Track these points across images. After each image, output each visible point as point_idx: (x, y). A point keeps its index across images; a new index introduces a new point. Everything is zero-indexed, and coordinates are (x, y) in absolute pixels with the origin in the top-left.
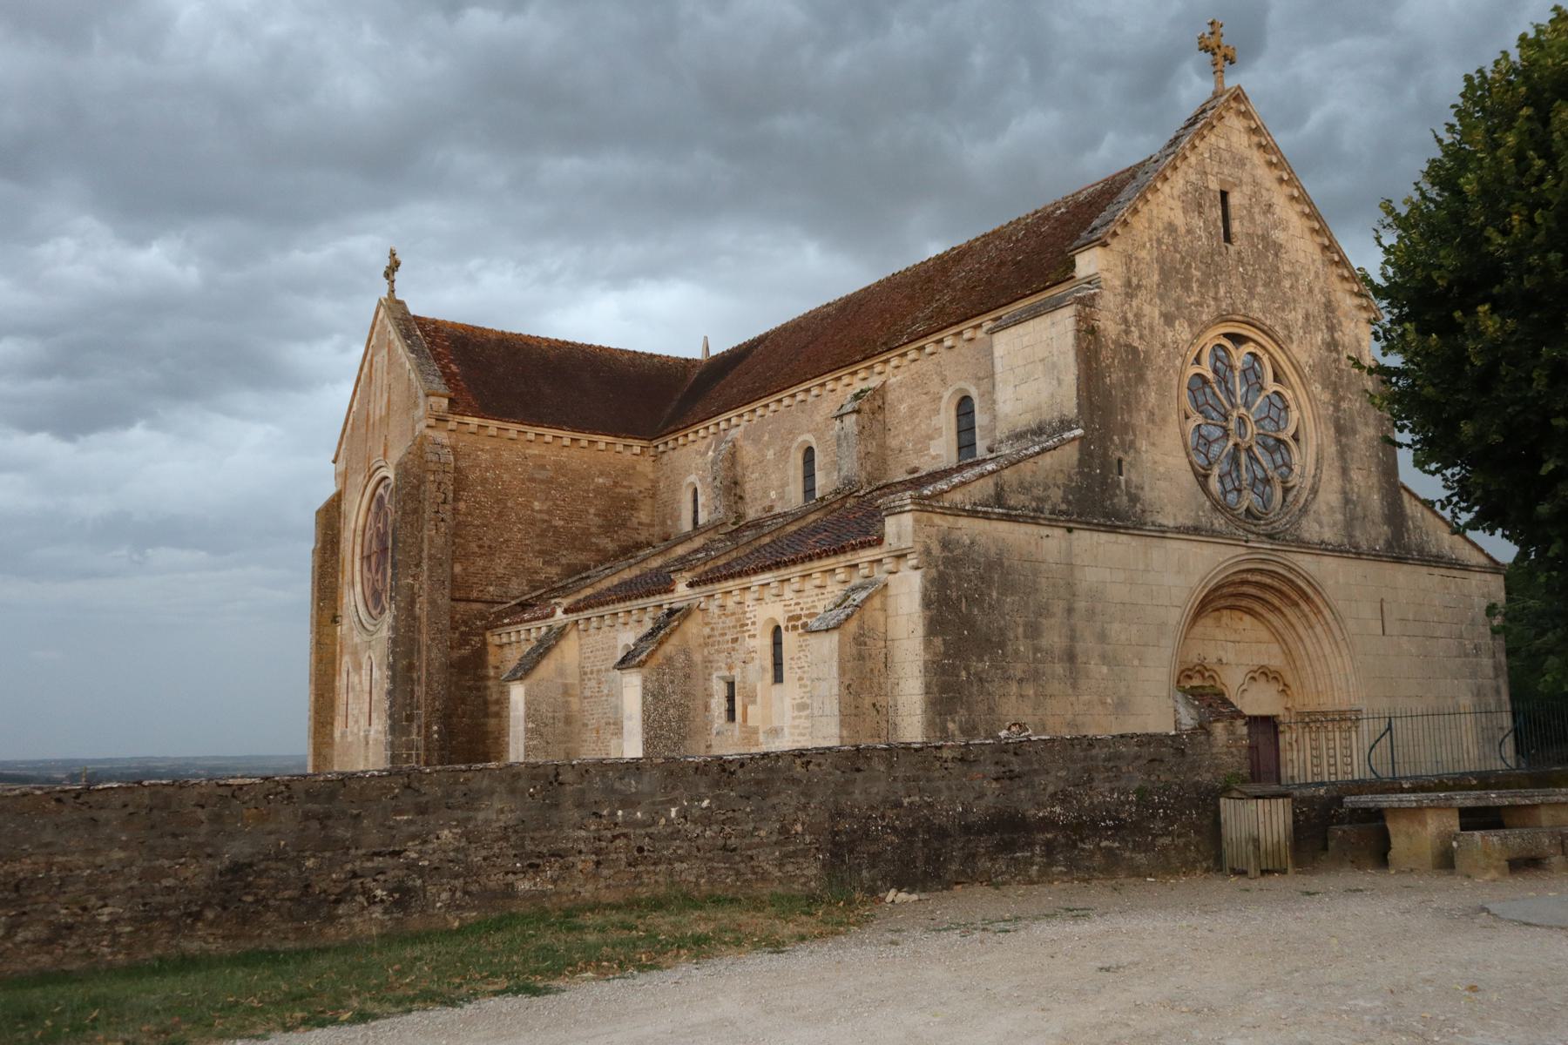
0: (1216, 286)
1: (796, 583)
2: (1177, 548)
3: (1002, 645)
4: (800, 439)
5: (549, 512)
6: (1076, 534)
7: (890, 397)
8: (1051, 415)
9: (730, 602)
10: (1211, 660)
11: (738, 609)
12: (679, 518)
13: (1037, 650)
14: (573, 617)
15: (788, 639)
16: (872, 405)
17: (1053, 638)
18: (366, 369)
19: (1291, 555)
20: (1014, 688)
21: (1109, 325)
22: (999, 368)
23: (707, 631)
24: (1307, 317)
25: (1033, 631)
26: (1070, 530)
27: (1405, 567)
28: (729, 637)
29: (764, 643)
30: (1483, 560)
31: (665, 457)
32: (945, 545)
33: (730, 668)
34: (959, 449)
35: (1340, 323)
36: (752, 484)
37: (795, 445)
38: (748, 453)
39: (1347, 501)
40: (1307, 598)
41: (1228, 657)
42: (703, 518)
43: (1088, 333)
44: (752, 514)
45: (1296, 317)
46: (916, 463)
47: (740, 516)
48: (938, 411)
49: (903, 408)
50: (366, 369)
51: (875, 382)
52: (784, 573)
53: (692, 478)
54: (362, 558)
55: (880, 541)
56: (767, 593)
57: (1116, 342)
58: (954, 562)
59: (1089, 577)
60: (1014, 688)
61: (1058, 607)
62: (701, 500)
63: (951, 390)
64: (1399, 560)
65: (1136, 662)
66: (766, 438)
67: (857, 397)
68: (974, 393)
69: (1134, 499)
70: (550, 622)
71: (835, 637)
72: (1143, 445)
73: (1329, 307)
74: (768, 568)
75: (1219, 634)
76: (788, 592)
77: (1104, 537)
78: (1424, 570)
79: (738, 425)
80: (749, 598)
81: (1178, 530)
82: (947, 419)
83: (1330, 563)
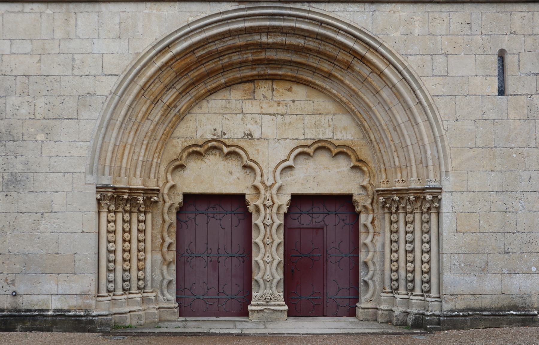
65: (41, 137)
75: (250, 107)
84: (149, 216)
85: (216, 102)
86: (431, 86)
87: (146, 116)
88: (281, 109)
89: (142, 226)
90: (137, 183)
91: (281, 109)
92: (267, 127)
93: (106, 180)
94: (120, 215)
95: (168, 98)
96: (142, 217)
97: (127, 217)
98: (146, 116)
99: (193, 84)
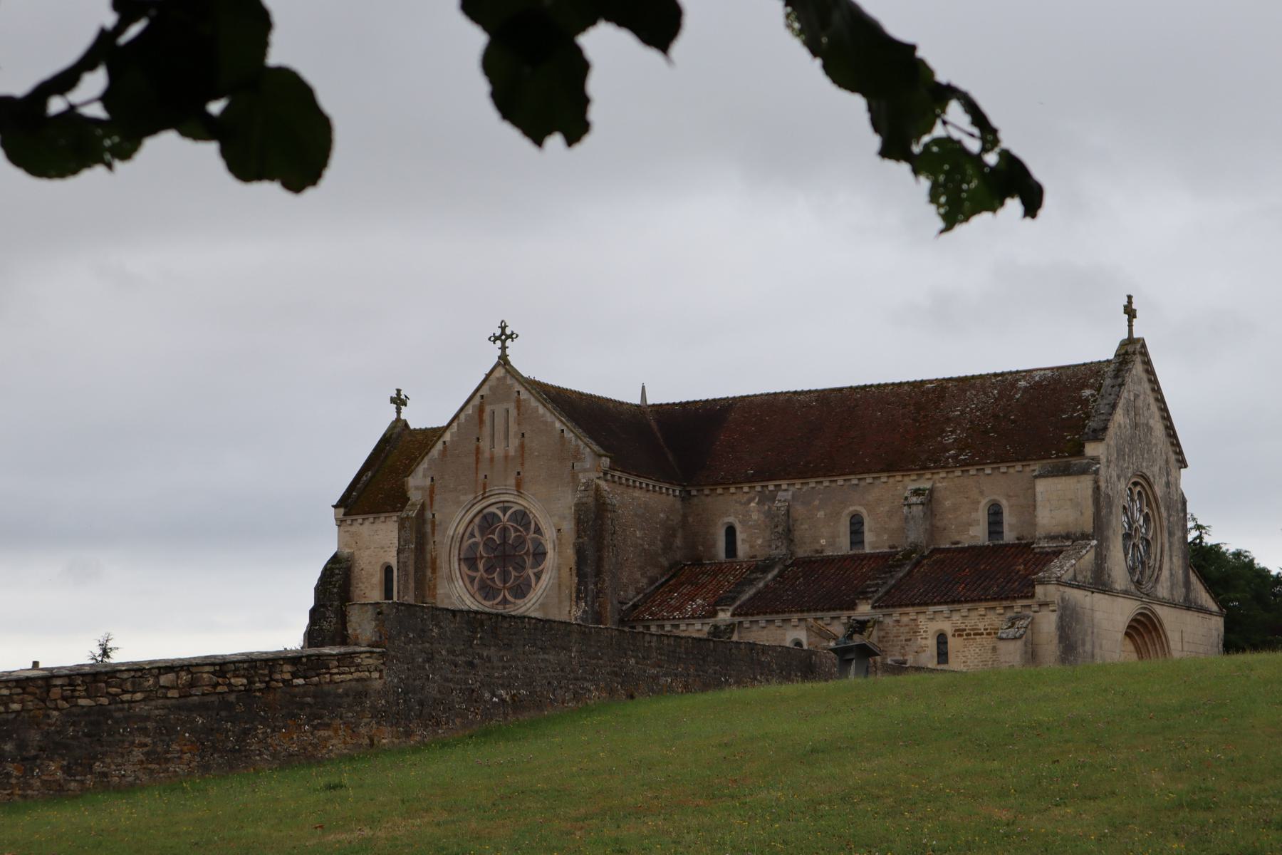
1: (964, 612)
4: (851, 509)
5: (642, 538)
7: (936, 495)
8: (1077, 530)
9: (905, 619)
11: (913, 623)
12: (714, 545)
14: (737, 619)
15: (953, 643)
16: (929, 499)
17: (1088, 647)
18: (470, 410)
21: (1103, 485)
22: (1039, 498)
23: (882, 633)
25: (1083, 644)
28: (903, 638)
29: (931, 643)
31: (696, 500)
32: (1063, 599)
33: (903, 655)
34: (990, 533)
36: (802, 530)
37: (847, 512)
38: (799, 510)
39: (1171, 575)
40: (1155, 628)
42: (742, 549)
43: (1097, 489)
44: (801, 553)
45: (1156, 469)
46: (957, 538)
47: (792, 554)
48: (977, 510)
49: (948, 503)
50: (470, 410)
51: (928, 485)
52: (957, 606)
53: (731, 519)
54: (460, 560)
55: (1033, 596)
56: (938, 616)
59: (1098, 616)
61: (1089, 631)
62: (740, 536)
63: (987, 500)
64: (1188, 608)
66: (817, 502)
67: (917, 492)
68: (1004, 503)
70: (712, 621)
71: (1020, 643)
73: (1167, 462)
74: (946, 603)
76: (956, 617)
79: (787, 491)
80: (922, 618)
82: (982, 516)
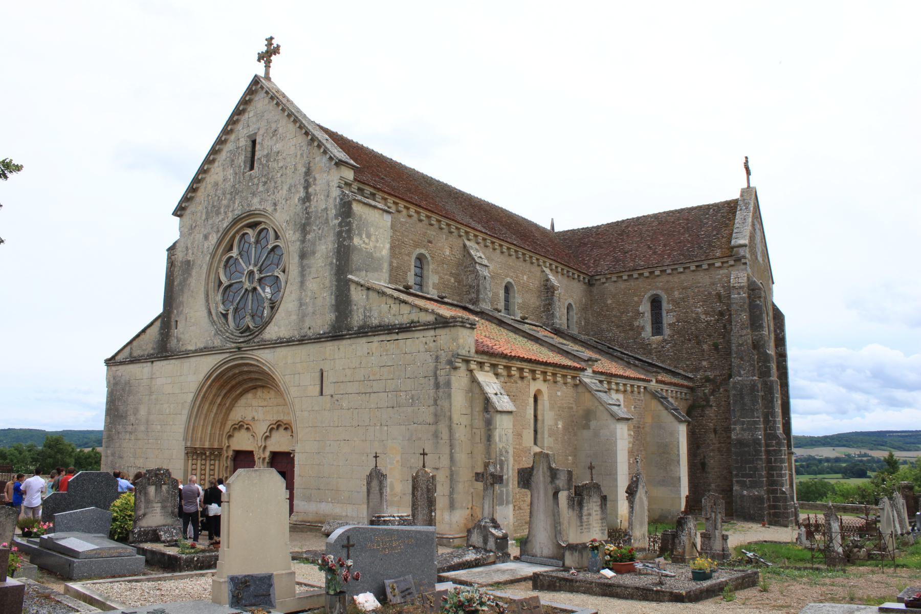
0: (234, 203)
2: (193, 361)
3: (126, 417)
6: (155, 363)
10: (249, 418)
13: (137, 419)
17: (143, 412)
19: (255, 352)
20: (128, 437)
24: (290, 189)
26: (152, 362)
27: (345, 342)
30: (430, 318)
35: (315, 179)
41: (259, 414)
57: (182, 262)
58: (116, 384)
60: (128, 437)
69: (178, 340)
72: (186, 310)
75: (255, 403)
77: (166, 362)
78: (364, 340)
81: (196, 351)
83: (282, 352)
84: (217, 462)
85: (242, 401)
86: (294, 392)
87: (209, 410)
88: (265, 403)
89: (212, 467)
90: (207, 445)
91: (265, 403)
92: (259, 414)
93: (189, 444)
94: (199, 462)
95: (219, 401)
96: (212, 462)
97: (203, 462)
98: (209, 410)
99: (229, 391)
